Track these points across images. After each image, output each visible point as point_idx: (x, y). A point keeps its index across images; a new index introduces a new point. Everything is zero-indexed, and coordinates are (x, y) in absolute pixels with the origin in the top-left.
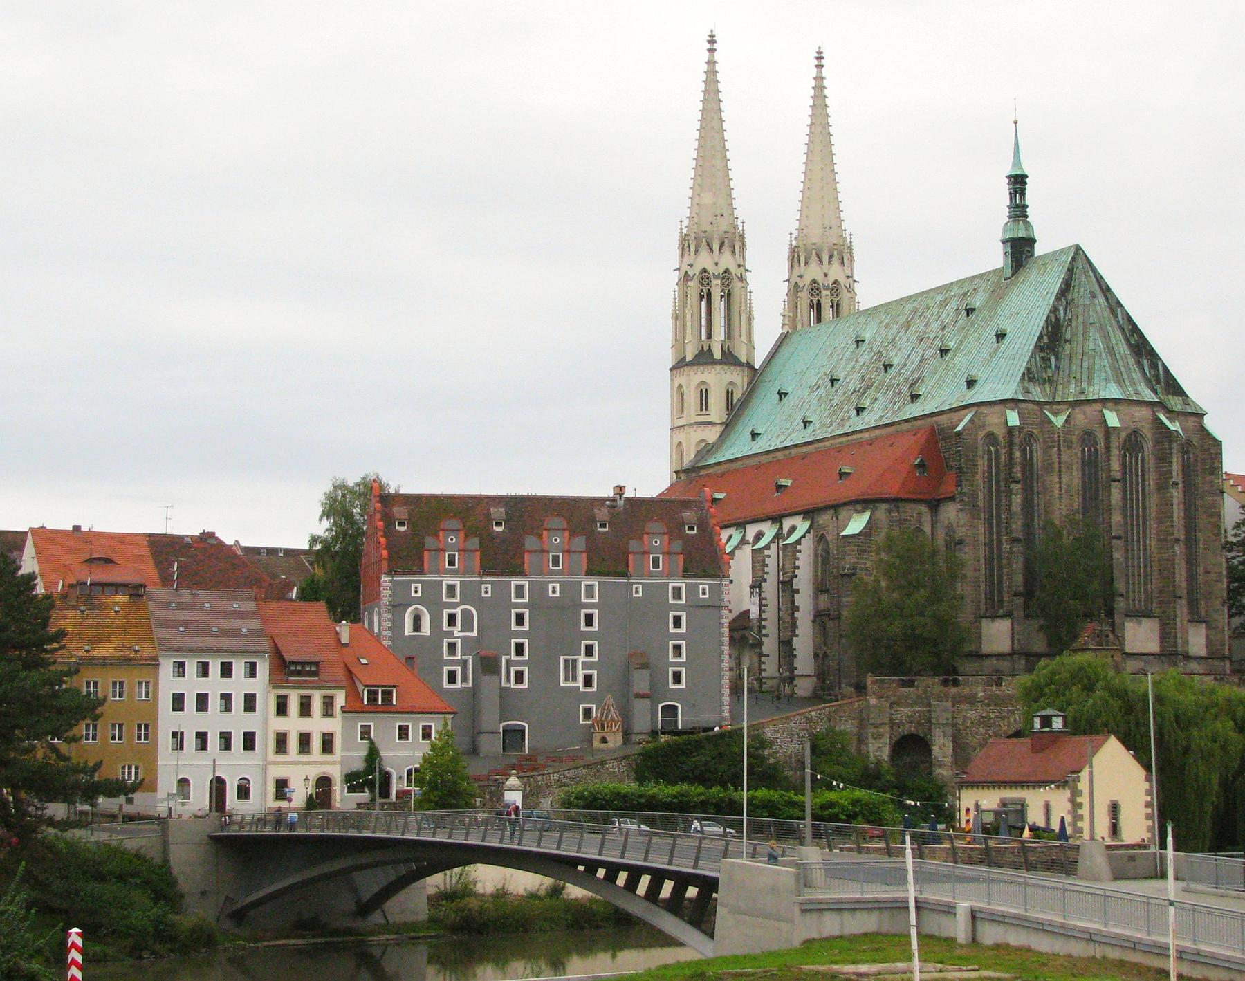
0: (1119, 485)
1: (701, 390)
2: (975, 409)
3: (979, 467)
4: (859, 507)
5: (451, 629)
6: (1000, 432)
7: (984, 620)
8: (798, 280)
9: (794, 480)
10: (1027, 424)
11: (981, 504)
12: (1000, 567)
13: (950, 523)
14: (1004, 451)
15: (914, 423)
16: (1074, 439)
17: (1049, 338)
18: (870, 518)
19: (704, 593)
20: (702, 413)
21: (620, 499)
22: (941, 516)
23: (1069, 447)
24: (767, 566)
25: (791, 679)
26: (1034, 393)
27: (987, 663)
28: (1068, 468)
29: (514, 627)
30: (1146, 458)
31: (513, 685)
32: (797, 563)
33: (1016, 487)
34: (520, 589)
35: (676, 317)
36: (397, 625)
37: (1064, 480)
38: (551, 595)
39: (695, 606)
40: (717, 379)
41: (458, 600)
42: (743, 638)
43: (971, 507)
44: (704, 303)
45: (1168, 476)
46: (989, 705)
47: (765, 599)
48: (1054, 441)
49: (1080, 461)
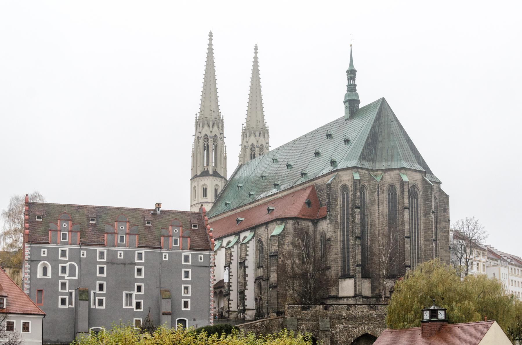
0: (407, 210)
1: (204, 188)
2: (336, 173)
4: (279, 222)
5: (63, 275)
6: (349, 184)
7: (340, 279)
8: (246, 144)
9: (245, 218)
10: (362, 180)
11: (339, 221)
12: (348, 252)
13: (323, 231)
14: (351, 193)
15: (304, 185)
16: (385, 188)
18: (284, 228)
19: (201, 259)
20: (204, 198)
21: (159, 210)
22: (319, 228)
23: (383, 193)
24: (233, 256)
25: (244, 311)
26: (365, 165)
27: (341, 302)
28: (382, 203)
29: (98, 275)
30: (419, 200)
31: (97, 307)
32: (248, 253)
33: (358, 210)
34: (102, 253)
35: (193, 156)
36: (33, 272)
37: (380, 208)
38: (119, 257)
39: (196, 266)
40: (210, 183)
41: (67, 259)
42: (221, 292)
43: (334, 222)
44: (205, 152)
45: (430, 208)
46: (348, 320)
48: (376, 189)
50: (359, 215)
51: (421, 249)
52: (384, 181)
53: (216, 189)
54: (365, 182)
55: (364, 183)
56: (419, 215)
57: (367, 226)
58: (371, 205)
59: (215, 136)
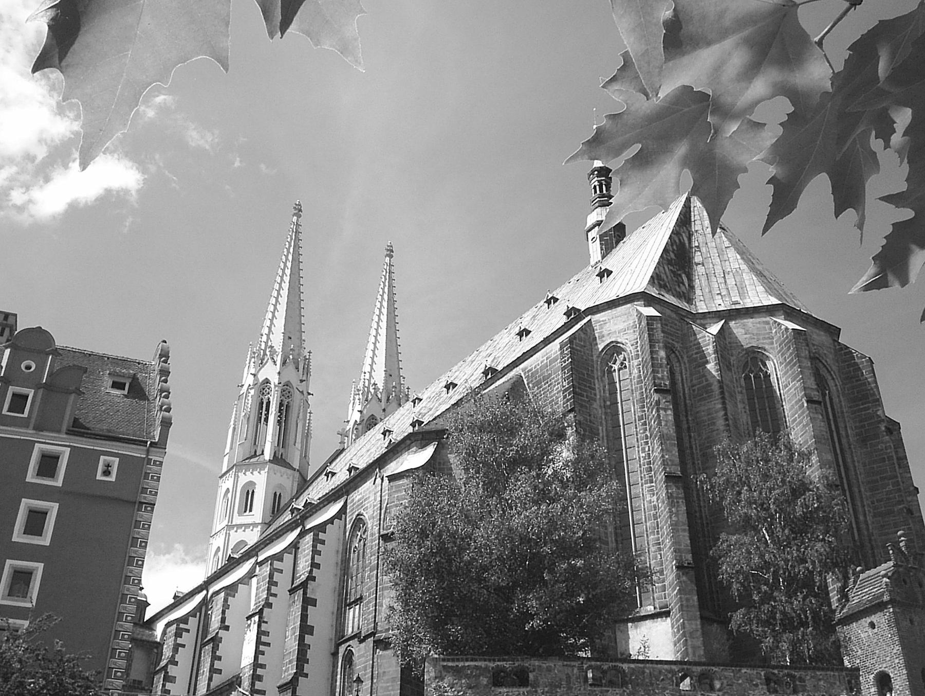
3: (597, 392)
14: (636, 362)
17: (675, 256)
19: (107, 473)
24: (276, 584)
28: (731, 396)
30: (836, 400)
37: (728, 406)
47: (266, 634)
49: (744, 391)
50: (669, 412)
51: (870, 540)
52: (728, 340)
53: (278, 494)
54: (673, 340)
55: (671, 341)
56: (844, 441)
57: (693, 458)
58: (700, 400)
59: (287, 384)
